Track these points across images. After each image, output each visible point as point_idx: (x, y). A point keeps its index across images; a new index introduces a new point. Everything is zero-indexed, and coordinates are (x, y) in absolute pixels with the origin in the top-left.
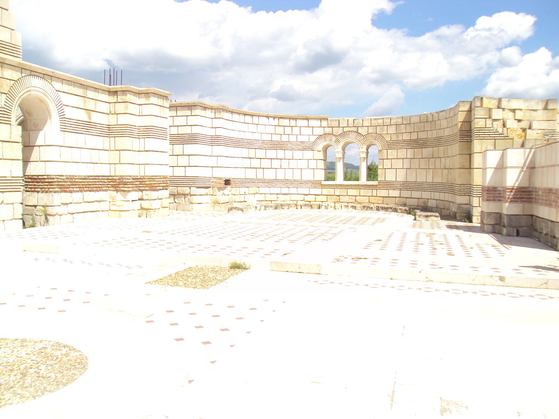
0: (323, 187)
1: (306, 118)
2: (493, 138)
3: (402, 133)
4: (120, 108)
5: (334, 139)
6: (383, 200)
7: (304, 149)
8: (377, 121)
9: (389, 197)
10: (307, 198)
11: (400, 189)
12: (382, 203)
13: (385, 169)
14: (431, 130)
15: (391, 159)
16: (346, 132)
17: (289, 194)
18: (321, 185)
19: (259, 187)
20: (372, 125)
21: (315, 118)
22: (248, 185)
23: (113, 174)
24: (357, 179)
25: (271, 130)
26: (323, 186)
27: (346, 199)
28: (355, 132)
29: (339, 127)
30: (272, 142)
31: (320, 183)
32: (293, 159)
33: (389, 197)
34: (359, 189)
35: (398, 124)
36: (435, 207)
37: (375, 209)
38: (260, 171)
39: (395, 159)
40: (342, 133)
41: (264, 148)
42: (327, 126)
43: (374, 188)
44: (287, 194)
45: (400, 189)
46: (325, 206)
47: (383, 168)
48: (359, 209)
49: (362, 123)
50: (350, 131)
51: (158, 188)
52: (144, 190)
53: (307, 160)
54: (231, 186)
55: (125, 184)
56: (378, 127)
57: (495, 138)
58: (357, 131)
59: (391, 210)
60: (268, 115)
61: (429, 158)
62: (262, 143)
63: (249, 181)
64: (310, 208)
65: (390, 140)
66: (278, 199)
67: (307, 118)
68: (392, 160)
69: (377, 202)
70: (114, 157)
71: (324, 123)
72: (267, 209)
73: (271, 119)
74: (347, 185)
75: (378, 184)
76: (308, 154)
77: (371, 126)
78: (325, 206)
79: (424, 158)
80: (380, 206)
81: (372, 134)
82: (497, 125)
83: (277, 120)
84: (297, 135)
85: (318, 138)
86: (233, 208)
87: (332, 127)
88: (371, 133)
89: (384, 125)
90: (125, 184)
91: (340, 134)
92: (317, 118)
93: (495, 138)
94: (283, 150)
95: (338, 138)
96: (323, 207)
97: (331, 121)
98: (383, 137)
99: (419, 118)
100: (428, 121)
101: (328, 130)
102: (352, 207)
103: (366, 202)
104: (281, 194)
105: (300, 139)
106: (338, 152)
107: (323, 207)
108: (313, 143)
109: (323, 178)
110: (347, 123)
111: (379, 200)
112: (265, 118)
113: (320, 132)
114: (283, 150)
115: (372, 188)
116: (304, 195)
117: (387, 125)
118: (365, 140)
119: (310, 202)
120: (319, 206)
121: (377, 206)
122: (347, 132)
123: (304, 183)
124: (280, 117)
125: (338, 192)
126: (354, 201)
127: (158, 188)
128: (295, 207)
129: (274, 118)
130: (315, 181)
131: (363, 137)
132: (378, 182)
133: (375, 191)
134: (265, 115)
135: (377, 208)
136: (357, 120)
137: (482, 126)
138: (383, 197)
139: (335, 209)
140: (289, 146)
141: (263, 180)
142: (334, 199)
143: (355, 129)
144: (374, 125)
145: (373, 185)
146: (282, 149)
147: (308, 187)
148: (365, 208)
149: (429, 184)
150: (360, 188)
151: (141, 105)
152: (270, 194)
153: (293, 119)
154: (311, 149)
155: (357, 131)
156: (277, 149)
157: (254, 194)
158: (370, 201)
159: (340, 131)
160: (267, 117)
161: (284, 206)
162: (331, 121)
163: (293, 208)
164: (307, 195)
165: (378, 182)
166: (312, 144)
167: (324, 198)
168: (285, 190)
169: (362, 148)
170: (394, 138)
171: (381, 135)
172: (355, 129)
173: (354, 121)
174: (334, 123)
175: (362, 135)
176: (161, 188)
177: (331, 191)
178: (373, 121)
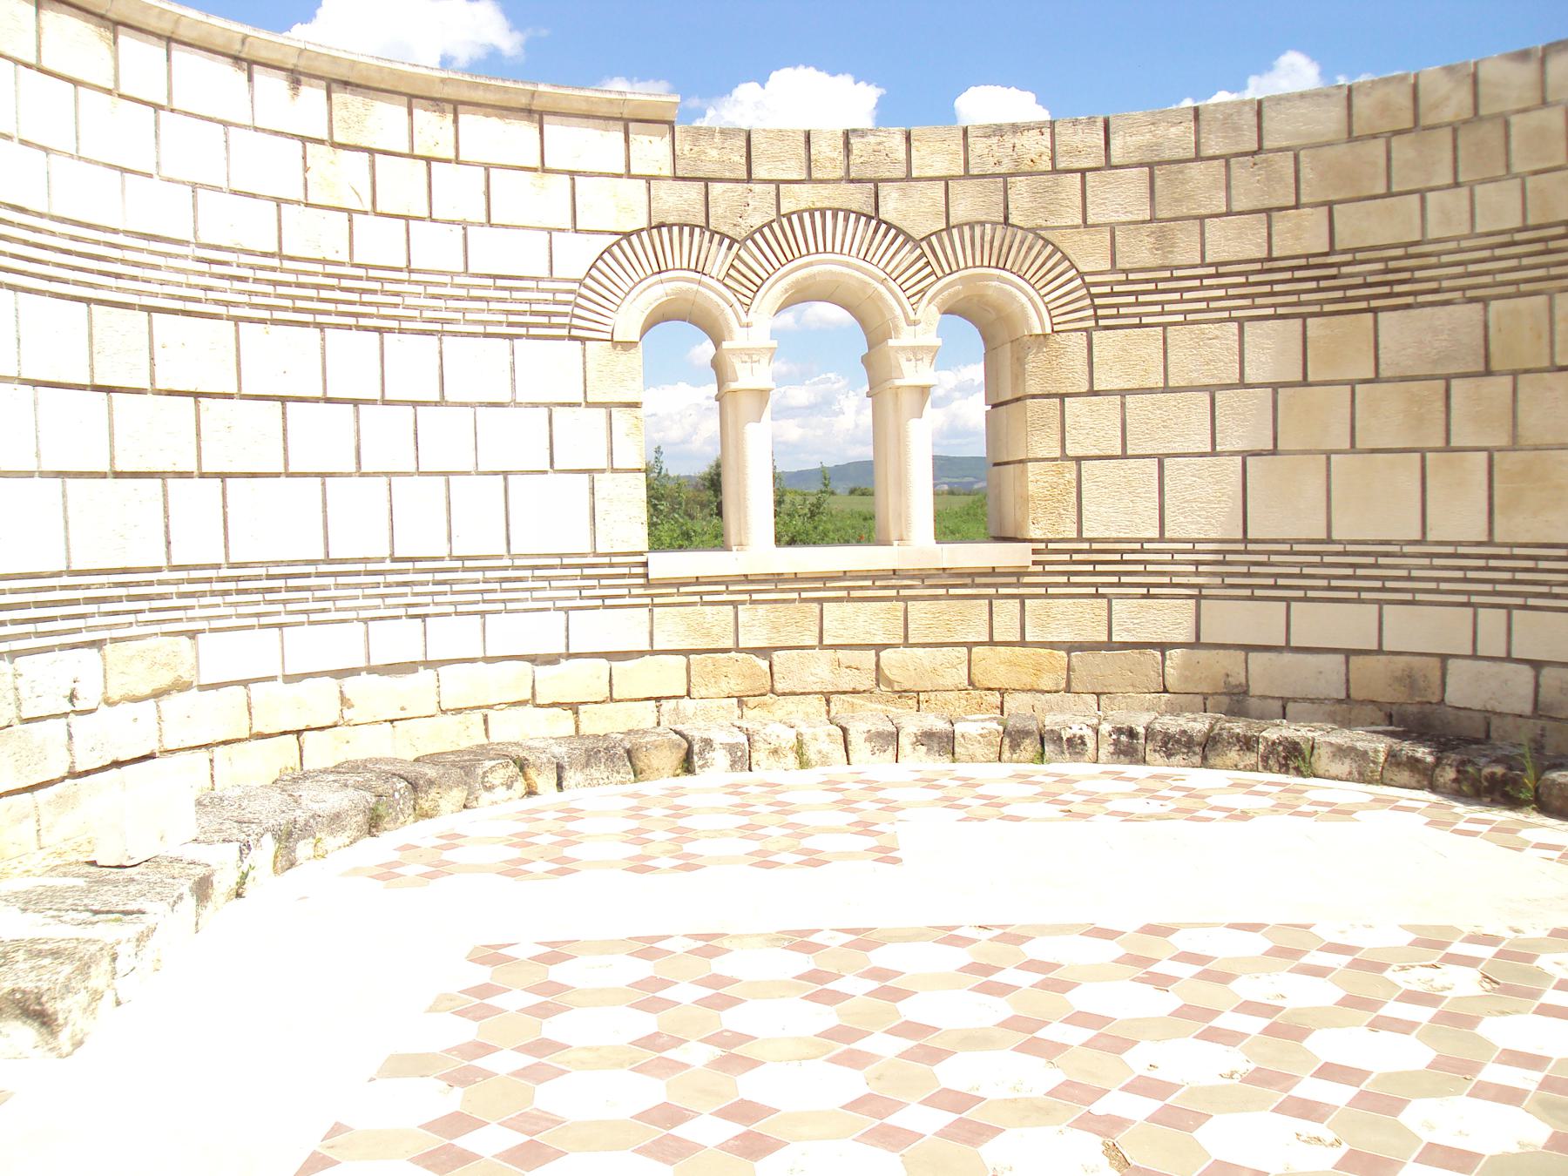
0: (657, 600)
1: (523, 101)
3: (1202, 218)
5: (719, 260)
6: (1069, 669)
7: (522, 331)
8: (1009, 140)
9: (1110, 645)
10: (558, 682)
11: (1194, 592)
12: (1063, 685)
13: (1078, 459)
14: (1457, 184)
15: (1123, 393)
16: (795, 218)
17: (428, 664)
18: (642, 581)
19: (192, 635)
20: (974, 171)
21: (583, 107)
22: (97, 623)
24: (864, 530)
26: (655, 591)
27: (819, 670)
28: (859, 215)
29: (749, 180)
30: (287, 264)
31: (641, 570)
32: (441, 403)
33: (1110, 645)
34: (898, 598)
35: (1167, 155)
36: (1527, 708)
37: (1106, 749)
38: (195, 498)
39: (1151, 391)
40: (769, 225)
41: (221, 310)
42: (668, 172)
43: (1002, 591)
44: (409, 667)
45: (1194, 592)
46: (731, 748)
47: (1065, 457)
48: (979, 751)
49: (902, 155)
50: (812, 212)
53: (545, 411)
56: (1020, 186)
58: (870, 211)
59: (1251, 758)
60: (244, 39)
61: (1447, 379)
62: (204, 267)
63: (100, 586)
64: (626, 772)
65: (1108, 267)
66: (348, 714)
67: (537, 105)
68: (1129, 398)
69: (1028, 680)
71: (652, 152)
72: (303, 849)
73: (271, 85)
74: (865, 578)
75: (1035, 563)
77: (967, 176)
78: (731, 748)
79: (1388, 380)
80: (1141, 730)
81: (978, 230)
83: (313, 94)
84: (465, 225)
85: (608, 250)
87: (707, 181)
88: (971, 226)
89: (1060, 166)
91: (760, 230)
92: (604, 110)
94: (366, 329)
95: (742, 253)
96: (720, 758)
97: (695, 141)
98: (1056, 249)
99: (1337, 112)
100: (1426, 120)
101: (679, 201)
102: (927, 738)
103: (949, 682)
104: (372, 670)
105: (492, 252)
107: (720, 758)
108: (575, 286)
109: (640, 540)
110: (802, 152)
111: (1038, 670)
112: (224, 67)
114: (366, 329)
115: (992, 591)
116: (533, 659)
117: (1083, 172)
118: (929, 270)
120: (682, 753)
121: (1119, 731)
122: (806, 216)
123: (528, 573)
124: (342, 73)
125: (757, 626)
126: (867, 682)
128: (520, 786)
129: (296, 78)
130: (606, 560)
131: (919, 251)
132: (1035, 552)
133: (1007, 611)
134: (219, 42)
135: (1116, 743)
136: (871, 139)
138: (1071, 647)
139: (804, 763)
140: (409, 301)
141: (224, 572)
142: (740, 673)
143: (857, 197)
144: (991, 169)
145: (993, 572)
146: (363, 322)
147: (559, 604)
148: (1029, 746)
149: (1455, 550)
150: (903, 592)
152: (289, 679)
153: (437, 103)
154: (564, 332)
155: (870, 211)
156: (321, 327)
157: (158, 695)
158: (978, 676)
159: (759, 210)
160: (237, 59)
161: (433, 793)
162: (695, 141)
163: (501, 792)
164: (552, 660)
165: (1035, 552)
166: (570, 297)
167: (666, 675)
168: (398, 640)
169: (915, 323)
170: (1139, 252)
171: (1043, 233)
172: (857, 197)
173: (847, 144)
174: (714, 153)
175: (909, 238)
177: (714, 623)
178: (978, 146)
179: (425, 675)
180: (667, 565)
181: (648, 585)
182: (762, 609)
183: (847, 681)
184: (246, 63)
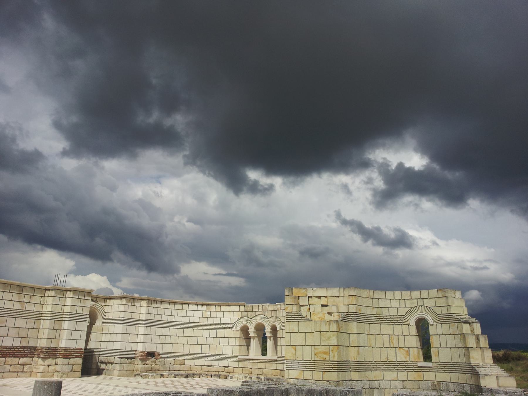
1: (228, 304)
2: (297, 320)
26: (240, 360)
30: (200, 323)
46: (231, 377)
51: (69, 356)
54: (155, 358)
57: (299, 320)
60: (196, 303)
67: (230, 304)
76: (229, 333)
78: (231, 377)
82: (304, 309)
85: (237, 320)
86: (137, 374)
93: (299, 320)
95: (252, 320)
96: (229, 377)
103: (270, 374)
105: (224, 321)
107: (229, 377)
127: (69, 356)
128: (206, 377)
132: (278, 358)
137: (290, 310)
161: (196, 376)
174: (249, 309)
176: (74, 356)
177: (245, 364)
179: (212, 367)
181: (239, 359)
182: (251, 363)
184: (197, 305)
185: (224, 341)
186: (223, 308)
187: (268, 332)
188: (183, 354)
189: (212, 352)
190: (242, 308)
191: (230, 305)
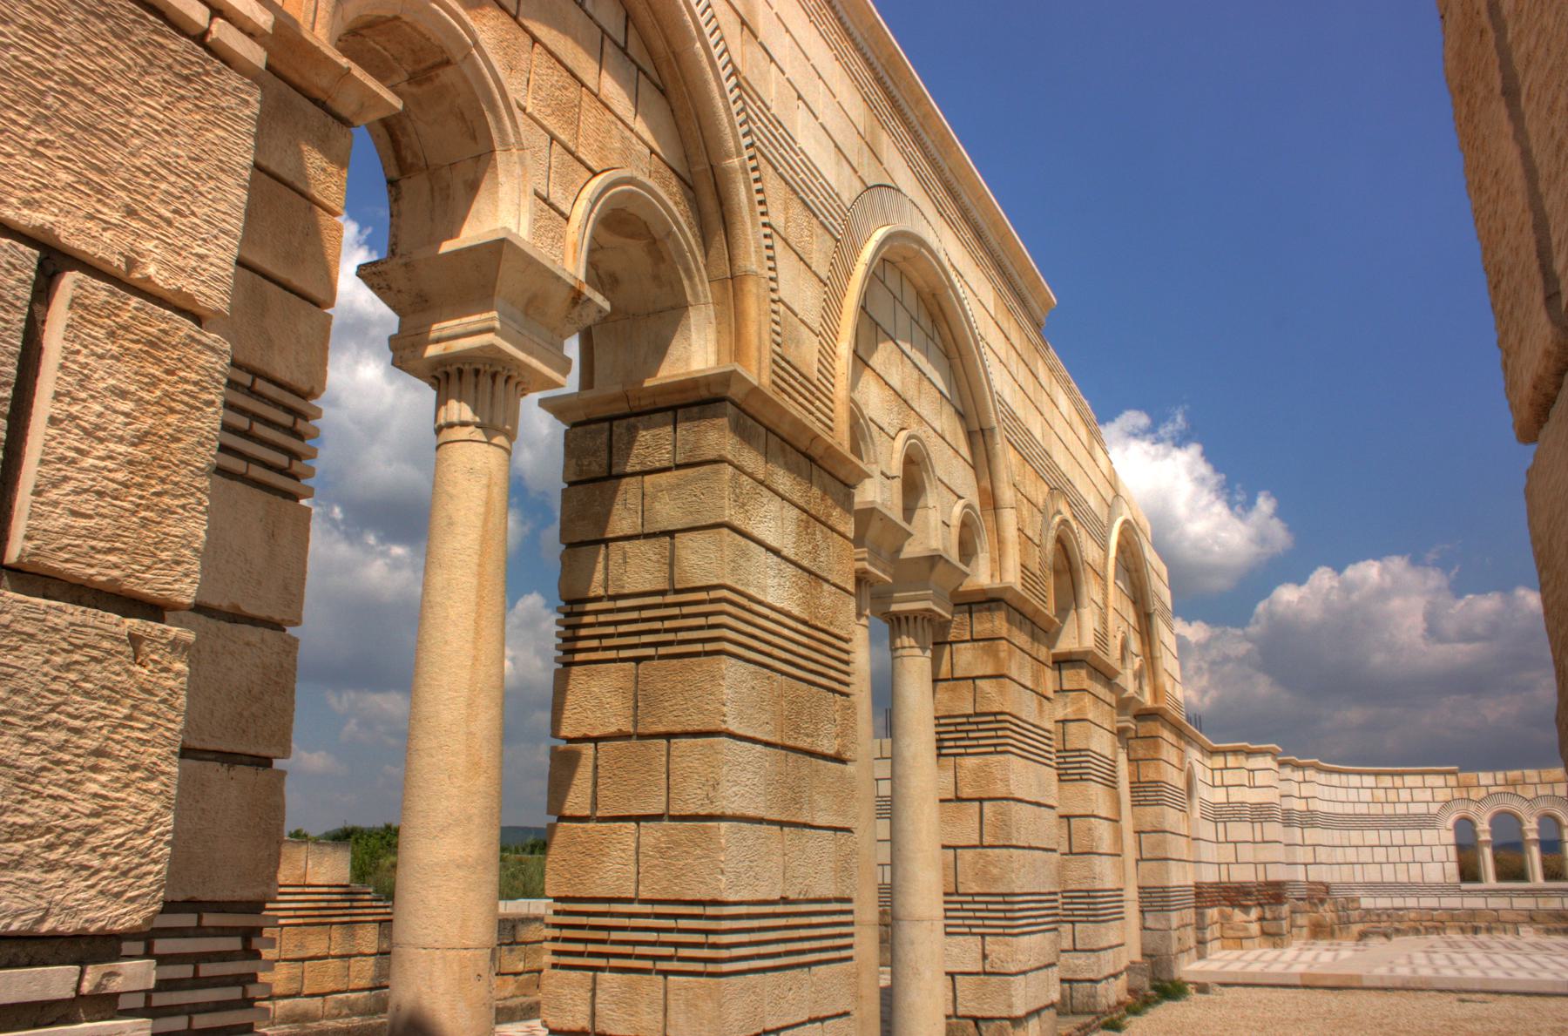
4: (1229, 777)
23: (1224, 878)
25: (1366, 795)
52: (1269, 904)
55: (1249, 894)
70: (1227, 853)
76: (1429, 835)
90: (1249, 894)
106: (1484, 831)
113: (1442, 795)
119: (1442, 922)
151: (1253, 771)
159: (1483, 792)
180: (1465, 886)
183: (1520, 919)
185: (1421, 853)
186: (1410, 780)
187: (1531, 830)
188: (1349, 886)
189: (1402, 878)
190: (1452, 780)
191: (1423, 773)
